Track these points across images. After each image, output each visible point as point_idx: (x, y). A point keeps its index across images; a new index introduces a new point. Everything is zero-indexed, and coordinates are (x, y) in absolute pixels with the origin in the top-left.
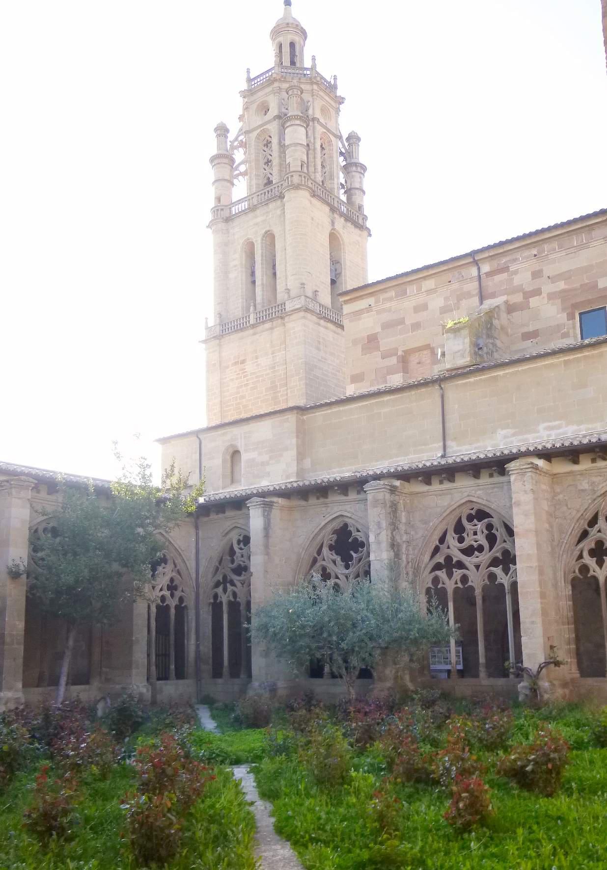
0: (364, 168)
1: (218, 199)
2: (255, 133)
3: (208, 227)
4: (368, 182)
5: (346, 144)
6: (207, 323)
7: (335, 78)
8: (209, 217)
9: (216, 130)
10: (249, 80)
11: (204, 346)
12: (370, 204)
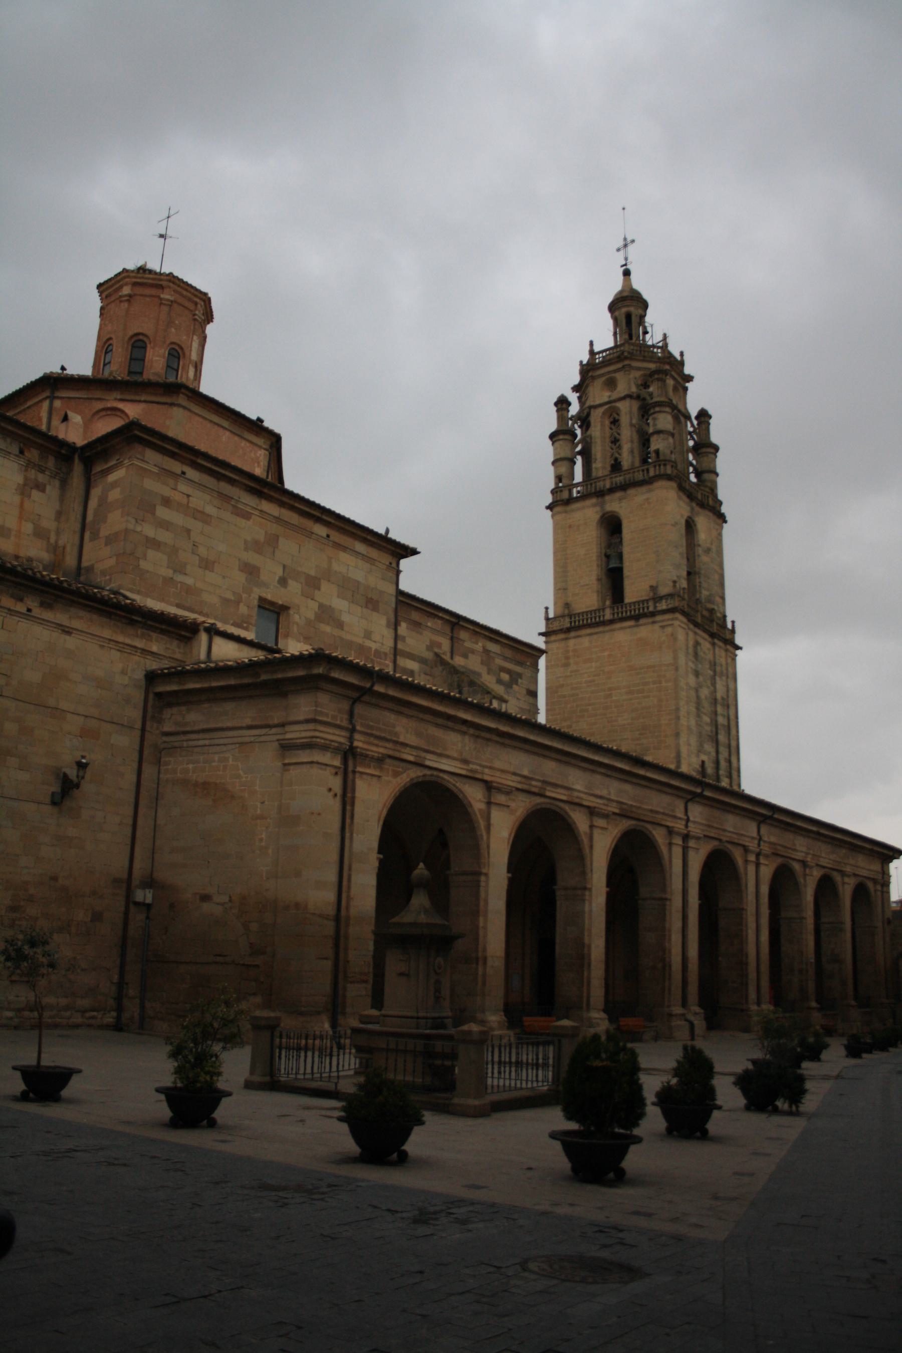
0: (716, 448)
1: (559, 478)
2: (601, 410)
3: (548, 507)
4: (722, 462)
7: (682, 354)
8: (549, 499)
9: (556, 404)
10: (592, 353)
12: (726, 490)
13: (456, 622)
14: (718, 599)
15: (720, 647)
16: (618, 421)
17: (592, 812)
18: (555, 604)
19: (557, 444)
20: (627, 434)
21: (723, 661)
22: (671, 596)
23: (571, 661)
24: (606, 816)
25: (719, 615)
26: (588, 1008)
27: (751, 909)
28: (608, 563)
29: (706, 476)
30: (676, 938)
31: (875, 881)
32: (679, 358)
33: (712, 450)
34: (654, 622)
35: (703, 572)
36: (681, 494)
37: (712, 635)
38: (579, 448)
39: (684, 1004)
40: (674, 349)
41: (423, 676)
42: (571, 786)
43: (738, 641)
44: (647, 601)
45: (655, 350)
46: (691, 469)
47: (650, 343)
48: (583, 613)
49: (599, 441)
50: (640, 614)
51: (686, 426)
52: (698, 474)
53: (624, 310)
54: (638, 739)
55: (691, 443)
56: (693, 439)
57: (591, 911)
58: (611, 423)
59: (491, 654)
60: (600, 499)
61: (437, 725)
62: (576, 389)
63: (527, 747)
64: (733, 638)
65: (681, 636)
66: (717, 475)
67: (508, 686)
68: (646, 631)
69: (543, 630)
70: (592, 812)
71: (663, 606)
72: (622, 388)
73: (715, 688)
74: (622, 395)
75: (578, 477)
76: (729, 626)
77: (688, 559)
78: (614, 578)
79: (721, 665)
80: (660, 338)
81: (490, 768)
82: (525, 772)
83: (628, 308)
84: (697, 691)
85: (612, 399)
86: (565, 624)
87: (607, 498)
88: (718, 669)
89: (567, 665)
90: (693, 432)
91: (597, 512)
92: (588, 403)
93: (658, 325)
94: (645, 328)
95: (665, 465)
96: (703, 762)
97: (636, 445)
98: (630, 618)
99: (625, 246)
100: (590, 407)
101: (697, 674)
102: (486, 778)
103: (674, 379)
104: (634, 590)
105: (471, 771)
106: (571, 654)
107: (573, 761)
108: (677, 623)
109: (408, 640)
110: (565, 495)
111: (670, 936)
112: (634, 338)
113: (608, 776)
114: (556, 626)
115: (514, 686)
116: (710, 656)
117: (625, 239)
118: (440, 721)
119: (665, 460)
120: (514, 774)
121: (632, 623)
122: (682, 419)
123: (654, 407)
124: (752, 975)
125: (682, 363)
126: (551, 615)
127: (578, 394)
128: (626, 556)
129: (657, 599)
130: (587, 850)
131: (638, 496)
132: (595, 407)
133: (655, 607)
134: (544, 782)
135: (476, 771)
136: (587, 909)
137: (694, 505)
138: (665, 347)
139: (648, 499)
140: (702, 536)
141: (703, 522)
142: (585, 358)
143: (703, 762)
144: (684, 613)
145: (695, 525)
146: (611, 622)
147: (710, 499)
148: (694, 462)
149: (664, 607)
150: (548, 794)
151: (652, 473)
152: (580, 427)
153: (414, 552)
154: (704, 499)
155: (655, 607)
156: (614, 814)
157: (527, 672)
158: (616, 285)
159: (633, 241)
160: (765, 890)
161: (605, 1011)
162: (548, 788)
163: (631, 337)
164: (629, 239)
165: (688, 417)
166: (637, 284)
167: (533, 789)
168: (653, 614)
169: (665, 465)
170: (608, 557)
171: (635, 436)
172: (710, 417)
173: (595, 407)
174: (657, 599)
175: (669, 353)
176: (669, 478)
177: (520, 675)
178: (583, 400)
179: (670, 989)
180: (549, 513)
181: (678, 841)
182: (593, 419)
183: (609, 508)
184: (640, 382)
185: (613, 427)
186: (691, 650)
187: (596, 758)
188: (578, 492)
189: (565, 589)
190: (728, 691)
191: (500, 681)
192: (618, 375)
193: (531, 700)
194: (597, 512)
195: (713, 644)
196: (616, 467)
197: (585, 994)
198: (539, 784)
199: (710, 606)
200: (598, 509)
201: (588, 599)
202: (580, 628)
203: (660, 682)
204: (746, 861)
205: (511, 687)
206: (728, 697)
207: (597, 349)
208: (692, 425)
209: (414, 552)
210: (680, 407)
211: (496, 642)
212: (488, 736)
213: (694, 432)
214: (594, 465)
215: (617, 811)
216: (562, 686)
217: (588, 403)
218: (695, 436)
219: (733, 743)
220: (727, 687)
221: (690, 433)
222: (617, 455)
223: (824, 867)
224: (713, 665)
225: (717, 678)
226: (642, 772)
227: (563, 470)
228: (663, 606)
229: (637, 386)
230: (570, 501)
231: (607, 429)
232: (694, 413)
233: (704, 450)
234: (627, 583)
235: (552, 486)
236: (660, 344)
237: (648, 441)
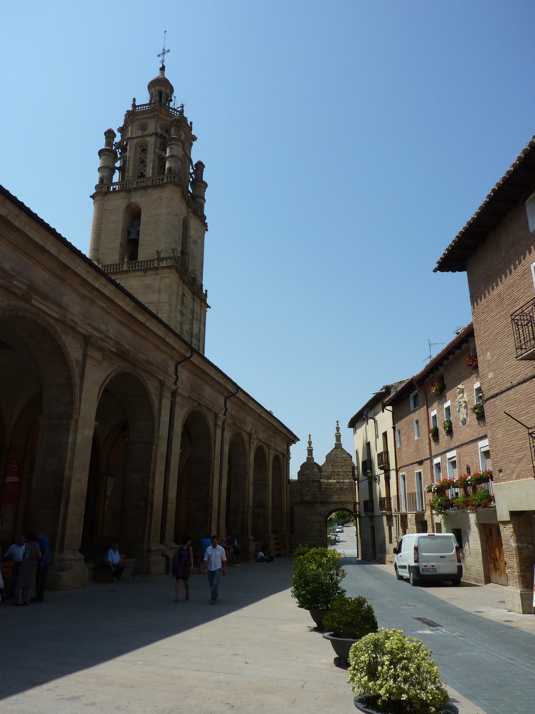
1: (102, 180)
2: (136, 141)
3: (91, 197)
4: (208, 194)
7: (191, 123)
10: (134, 106)
14: (198, 273)
15: (198, 303)
16: (146, 149)
17: (86, 341)
19: (103, 157)
20: (150, 156)
21: (198, 311)
22: (170, 258)
24: (102, 350)
26: (61, 550)
27: (217, 462)
30: (159, 480)
31: (284, 455)
34: (157, 274)
35: (191, 254)
36: (183, 199)
37: (194, 293)
39: (162, 540)
43: (208, 301)
44: (153, 260)
48: (108, 266)
49: (132, 160)
50: (148, 268)
53: (157, 88)
57: (75, 442)
58: (141, 151)
60: (128, 194)
62: (121, 130)
65: (175, 286)
68: (150, 279)
70: (86, 341)
71: (164, 264)
72: (151, 128)
73: (192, 327)
76: (204, 292)
77: (182, 245)
78: (131, 245)
79: (197, 314)
87: (133, 194)
88: (195, 315)
90: (193, 173)
91: (125, 202)
95: (174, 177)
98: (141, 270)
99: (164, 53)
101: (182, 314)
104: (144, 254)
108: (171, 275)
110: (105, 189)
111: (154, 477)
116: (191, 306)
117: (164, 50)
121: (141, 273)
124: (215, 515)
125: (191, 129)
129: (160, 259)
130: (77, 380)
131: (155, 194)
133: (158, 264)
136: (70, 440)
138: (182, 112)
139: (160, 197)
140: (192, 232)
141: (193, 223)
144: (177, 270)
145: (189, 224)
146: (127, 272)
149: (165, 265)
150: (34, 302)
151: (165, 181)
155: (158, 264)
156: (110, 351)
160: (226, 448)
161: (81, 551)
164: (166, 49)
165: (191, 161)
166: (168, 75)
167: (15, 290)
168: (156, 269)
169: (174, 177)
170: (129, 232)
174: (160, 259)
176: (176, 185)
179: (150, 526)
181: (167, 394)
183: (133, 200)
185: (142, 153)
186: (180, 297)
188: (114, 189)
190: (200, 331)
192: (149, 121)
194: (125, 202)
195: (194, 299)
196: (142, 175)
197: (59, 533)
198: (25, 288)
199: (193, 276)
200: (126, 200)
204: (216, 424)
206: (199, 334)
207: (137, 104)
208: (193, 168)
210: (187, 152)
214: (126, 174)
215: (114, 350)
218: (193, 175)
220: (200, 328)
222: (143, 171)
223: (260, 440)
224: (192, 312)
225: (194, 321)
226: (141, 318)
227: (105, 174)
228: (164, 264)
230: (107, 193)
233: (199, 184)
234: (140, 248)
236: (179, 109)
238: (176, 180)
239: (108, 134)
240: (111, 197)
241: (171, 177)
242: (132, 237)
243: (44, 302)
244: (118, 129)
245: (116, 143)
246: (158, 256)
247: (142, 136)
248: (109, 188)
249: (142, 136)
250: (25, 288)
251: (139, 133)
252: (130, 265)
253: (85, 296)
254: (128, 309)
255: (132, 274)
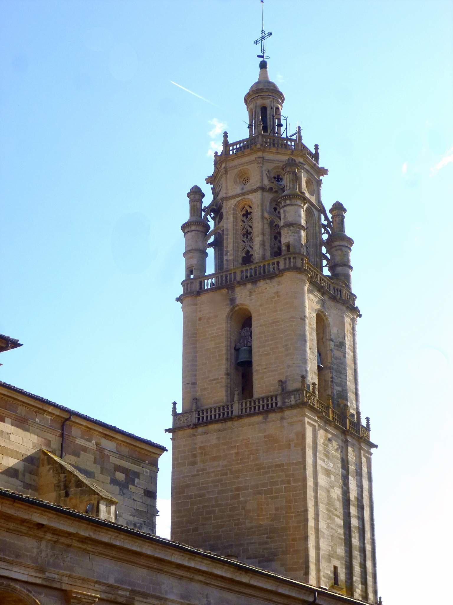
0: (350, 241)
1: (190, 271)
2: (233, 202)
3: (178, 300)
4: (355, 257)
5: (330, 216)
6: (174, 409)
8: (180, 291)
10: (226, 144)
11: (171, 435)
12: (359, 283)
13: (66, 421)
16: (251, 213)
18: (183, 399)
19: (189, 234)
20: (258, 225)
23: (198, 459)
25: (352, 411)
28: (237, 358)
29: (339, 269)
32: (314, 151)
33: (346, 244)
35: (335, 367)
37: (344, 432)
38: (212, 239)
40: (309, 143)
41: (28, 475)
42: (164, 596)
43: (373, 439)
45: (289, 143)
46: (324, 262)
47: (284, 136)
51: (320, 219)
52: (332, 268)
53: (259, 102)
54: (266, 543)
55: (325, 237)
56: (328, 232)
59: (106, 452)
61: (8, 530)
62: (210, 180)
63: (113, 553)
64: (368, 436)
66: (351, 268)
67: (123, 486)
69: (170, 426)
72: (255, 181)
74: (255, 187)
75: (210, 268)
76: (364, 423)
80: (295, 130)
81: (70, 576)
82: (111, 581)
83: (264, 102)
84: (328, 491)
85: (244, 191)
86: (192, 420)
87: (238, 290)
89: (194, 463)
92: (220, 197)
93: (293, 117)
94: (279, 120)
95: (294, 258)
96: (335, 568)
97: (267, 237)
99: (263, 38)
100: (222, 199)
102: (64, 588)
103: (307, 171)
105: (47, 580)
106: (198, 451)
107: (166, 569)
109: (13, 438)
112: (269, 131)
113: (207, 584)
114: (184, 421)
115: (131, 486)
117: (263, 32)
118: (11, 525)
119: (295, 253)
120: (97, 582)
121: (259, 418)
122: (316, 213)
123: (285, 200)
125: (316, 156)
126: (179, 410)
127: (212, 186)
128: (254, 350)
131: (267, 288)
132: (227, 198)
133: (284, 403)
134: (132, 591)
135: (53, 580)
137: (326, 298)
140: (334, 331)
142: (220, 149)
143: (335, 568)
146: (239, 417)
147: (343, 293)
148: (328, 255)
149: (293, 402)
151: (282, 266)
152: (212, 218)
153: (15, 344)
154: (338, 294)
155: (284, 403)
157: (146, 471)
158: (253, 77)
159: (270, 34)
162: (137, 598)
163: (265, 129)
165: (322, 210)
169: (294, 258)
170: (237, 350)
171: (267, 230)
172: (345, 210)
173: (227, 198)
175: (303, 145)
177: (137, 475)
178: (217, 190)
180: (179, 304)
182: (224, 211)
184: (272, 176)
185: (244, 219)
187: (192, 564)
189: (194, 384)
191: (114, 481)
193: (148, 501)
195: (346, 442)
196: (247, 259)
198: (128, 594)
201: (217, 395)
202: (207, 423)
203: (289, 482)
205: (128, 488)
207: (230, 141)
208: (326, 218)
209: (15, 344)
211: (112, 438)
212: (68, 541)
213: (329, 225)
214: (225, 258)
216: (188, 486)
217: (222, 195)
219: (368, 547)
221: (324, 226)
226: (245, 579)
227: (194, 261)
229: (269, 178)
231: (239, 221)
232: (328, 207)
233: (337, 243)
235: (184, 278)
236: (294, 137)
237: (280, 233)
238: (299, 264)
239: (192, 196)
240: (204, 298)
241: (290, 259)
242: (243, 357)
243: (145, 600)
244: (206, 179)
245: (205, 207)
246: (283, 389)
247: (243, 194)
248: (201, 284)
249: (243, 194)
250: (128, 594)
251: (238, 191)
252: (242, 406)
253: (182, 576)
254: (228, 575)
255: (246, 420)
